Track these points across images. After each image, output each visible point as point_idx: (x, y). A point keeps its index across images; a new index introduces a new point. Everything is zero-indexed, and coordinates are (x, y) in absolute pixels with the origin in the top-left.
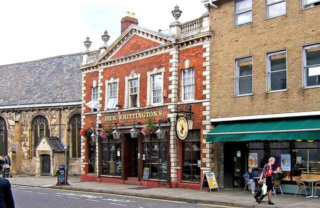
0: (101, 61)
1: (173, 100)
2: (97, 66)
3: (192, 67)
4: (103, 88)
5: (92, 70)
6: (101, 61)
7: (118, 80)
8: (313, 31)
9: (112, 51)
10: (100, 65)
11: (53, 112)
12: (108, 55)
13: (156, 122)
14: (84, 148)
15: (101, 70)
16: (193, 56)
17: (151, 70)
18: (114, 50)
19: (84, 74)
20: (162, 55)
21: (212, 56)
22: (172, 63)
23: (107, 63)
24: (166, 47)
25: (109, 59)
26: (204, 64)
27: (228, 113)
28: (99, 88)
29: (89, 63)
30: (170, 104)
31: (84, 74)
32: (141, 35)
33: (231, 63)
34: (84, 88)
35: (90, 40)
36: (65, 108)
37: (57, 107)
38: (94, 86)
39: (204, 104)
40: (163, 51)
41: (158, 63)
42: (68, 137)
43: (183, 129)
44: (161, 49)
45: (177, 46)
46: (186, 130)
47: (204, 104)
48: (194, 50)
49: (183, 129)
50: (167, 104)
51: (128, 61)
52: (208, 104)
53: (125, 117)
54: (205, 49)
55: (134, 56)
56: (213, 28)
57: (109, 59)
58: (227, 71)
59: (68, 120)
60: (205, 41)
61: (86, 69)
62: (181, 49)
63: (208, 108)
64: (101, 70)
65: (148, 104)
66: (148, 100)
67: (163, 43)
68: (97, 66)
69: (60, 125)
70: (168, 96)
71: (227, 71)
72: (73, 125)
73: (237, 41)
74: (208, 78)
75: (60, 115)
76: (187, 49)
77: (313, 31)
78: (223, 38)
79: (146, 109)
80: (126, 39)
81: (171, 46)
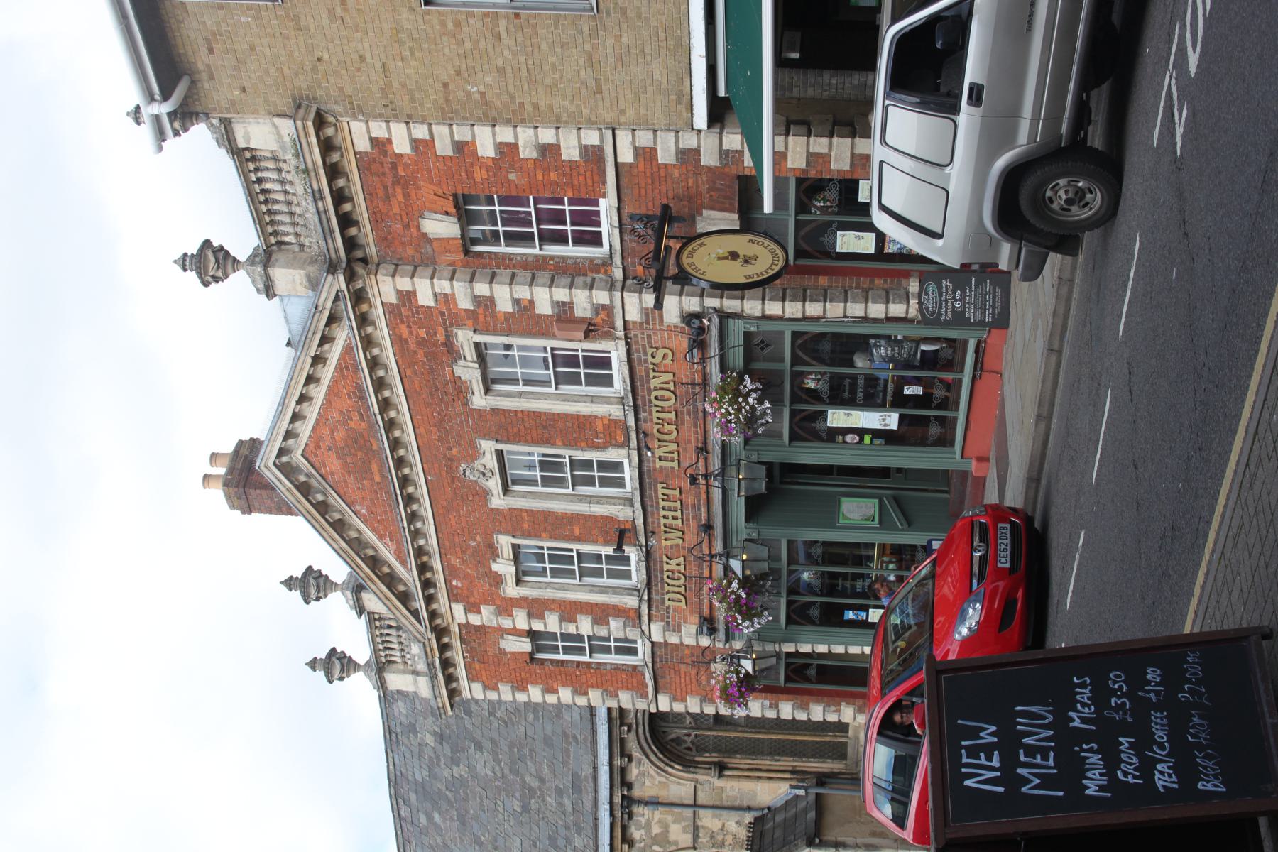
0: (415, 614)
1: (602, 297)
2: (440, 632)
3: (457, 205)
4: (536, 608)
5: (458, 655)
6: (415, 614)
7: (505, 542)
9: (374, 562)
10: (433, 615)
11: (636, 834)
12: (390, 580)
13: (698, 379)
14: (805, 707)
15: (458, 614)
16: (406, 196)
17: (461, 390)
18: (370, 552)
19: (472, 690)
20: (397, 340)
21: (407, 110)
22: (435, 294)
23: (427, 584)
24: (363, 320)
25: (409, 576)
26: (444, 147)
28: (537, 626)
29: (422, 666)
30: (618, 311)
31: (472, 690)
32: (305, 430)
33: (443, 24)
34: (535, 693)
35: (322, 655)
36: (621, 779)
37: (618, 814)
38: (525, 645)
39: (627, 156)
40: (383, 333)
41: (431, 356)
42: (754, 773)
43: (734, 256)
44: (368, 342)
45: (360, 269)
46: (741, 243)
47: (627, 156)
48: (381, 193)
49: (734, 256)
50: (619, 324)
51: (421, 489)
52: (624, 139)
53: (667, 516)
54: (375, 142)
55: (400, 463)
56: (285, 104)
57: (409, 576)
58: (476, 44)
59: (676, 770)
60: (338, 141)
61: (450, 679)
62: (372, 250)
63: (644, 139)
64: (458, 614)
65: (616, 411)
66: (599, 410)
67: (344, 335)
68: (440, 632)
69: (695, 805)
70: (582, 320)
71: (476, 44)
72: (701, 750)
74: (505, 134)
75: (654, 803)
76: (375, 223)
78: (326, 56)
79: (637, 420)
80: (320, 497)
81: (359, 297)
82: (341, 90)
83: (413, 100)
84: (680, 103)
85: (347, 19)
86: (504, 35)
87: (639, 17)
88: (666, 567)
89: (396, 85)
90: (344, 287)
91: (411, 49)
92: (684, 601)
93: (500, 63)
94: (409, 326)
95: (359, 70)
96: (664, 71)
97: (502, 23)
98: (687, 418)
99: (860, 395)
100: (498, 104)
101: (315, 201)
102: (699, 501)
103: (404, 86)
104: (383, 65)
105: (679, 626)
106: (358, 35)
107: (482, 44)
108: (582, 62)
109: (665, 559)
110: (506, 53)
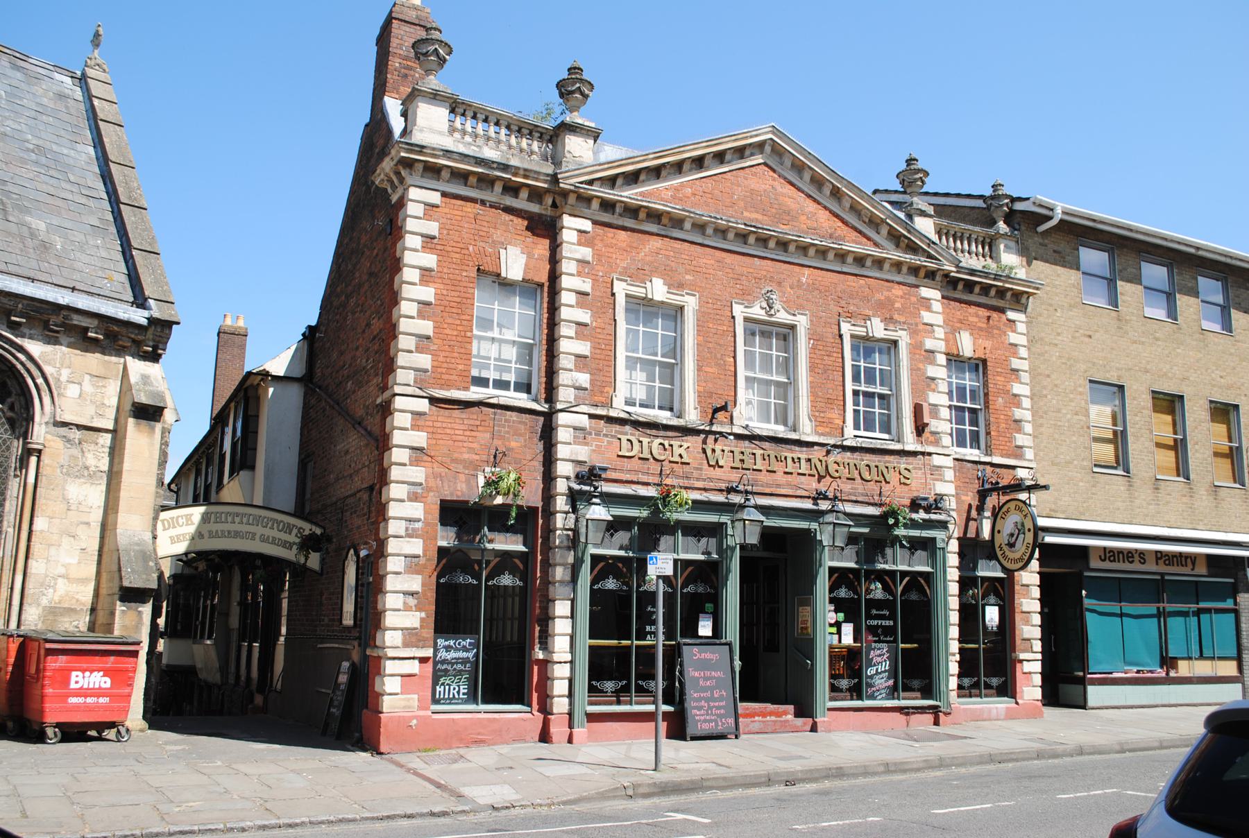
0: (591, 182)
8: (1221, 377)
16: (981, 329)
25: (628, 195)
27: (1081, 509)
58: (1071, 401)
73: (1090, 337)
77: (1221, 377)
81: (931, 275)
82: (1040, 315)
83: (1039, 355)
84: (1050, 510)
85: (1077, 335)
86: (1077, 417)
87: (1093, 494)
88: (675, 443)
89: (1047, 348)
90: (946, 267)
91: (1065, 363)
92: (627, 454)
93: (1064, 411)
94: (902, 297)
95: (1052, 330)
96: (1067, 504)
97: (1084, 418)
98: (849, 486)
99: (875, 622)
100: (1042, 404)
101: (996, 275)
102: (762, 486)
103: (1046, 352)
104: (1056, 345)
105: (586, 444)
106: (1070, 337)
107: (1073, 404)
108: (1068, 457)
109: (685, 445)
110: (1069, 416)
